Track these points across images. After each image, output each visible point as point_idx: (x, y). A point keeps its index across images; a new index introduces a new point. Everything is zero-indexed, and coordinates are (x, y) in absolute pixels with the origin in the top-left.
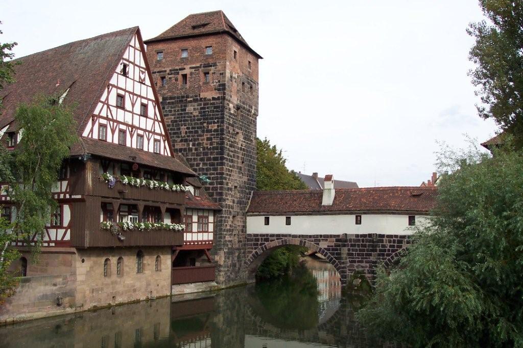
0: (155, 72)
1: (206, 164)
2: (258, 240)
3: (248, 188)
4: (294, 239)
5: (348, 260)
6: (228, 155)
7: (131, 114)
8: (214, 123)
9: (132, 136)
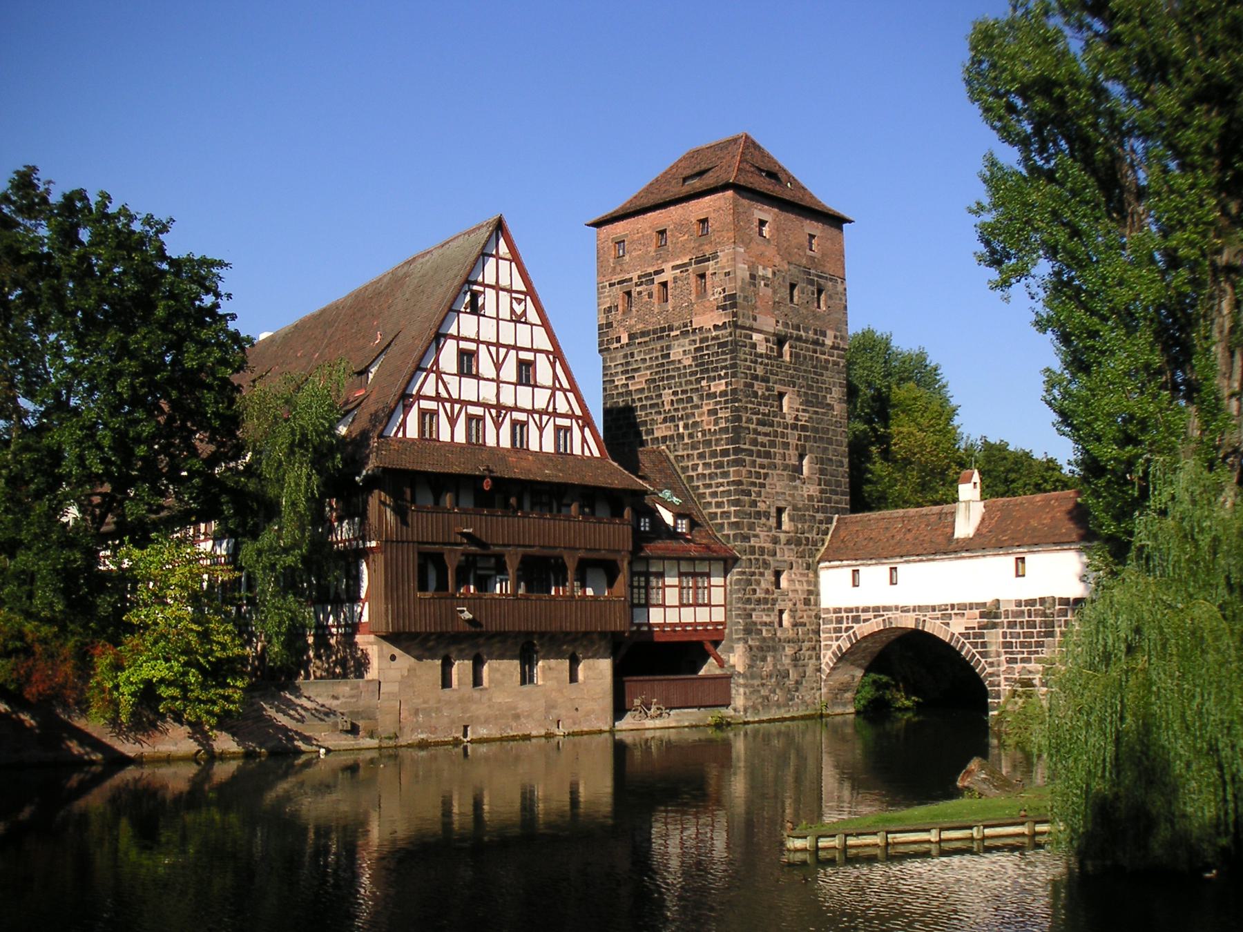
0: (614, 284)
1: (706, 465)
2: (840, 621)
3: (824, 510)
4: (904, 614)
5: (1003, 658)
6: (754, 442)
7: (495, 384)
8: (720, 378)
9: (498, 426)
